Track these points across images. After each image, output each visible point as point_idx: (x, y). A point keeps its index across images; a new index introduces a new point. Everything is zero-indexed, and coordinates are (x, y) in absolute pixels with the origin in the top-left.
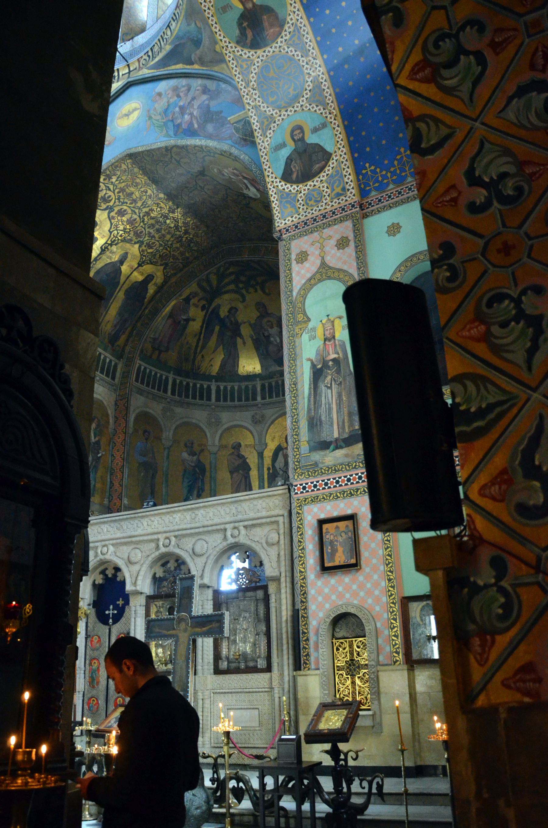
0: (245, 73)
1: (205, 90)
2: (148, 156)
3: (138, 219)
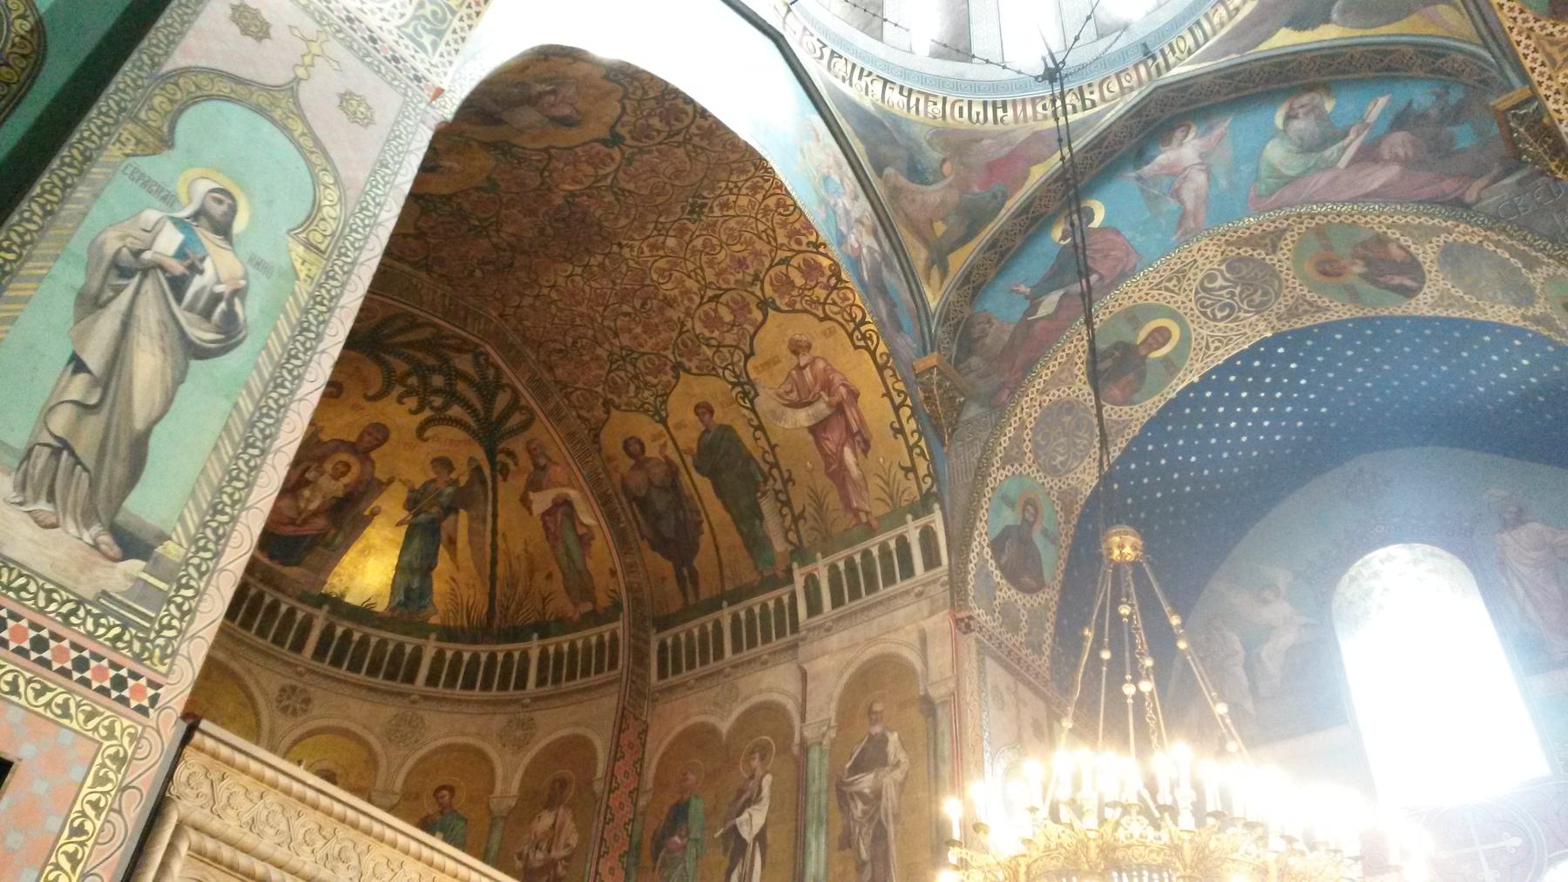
0: (1056, 381)
1: (875, 234)
2: (778, 205)
3: (578, 187)
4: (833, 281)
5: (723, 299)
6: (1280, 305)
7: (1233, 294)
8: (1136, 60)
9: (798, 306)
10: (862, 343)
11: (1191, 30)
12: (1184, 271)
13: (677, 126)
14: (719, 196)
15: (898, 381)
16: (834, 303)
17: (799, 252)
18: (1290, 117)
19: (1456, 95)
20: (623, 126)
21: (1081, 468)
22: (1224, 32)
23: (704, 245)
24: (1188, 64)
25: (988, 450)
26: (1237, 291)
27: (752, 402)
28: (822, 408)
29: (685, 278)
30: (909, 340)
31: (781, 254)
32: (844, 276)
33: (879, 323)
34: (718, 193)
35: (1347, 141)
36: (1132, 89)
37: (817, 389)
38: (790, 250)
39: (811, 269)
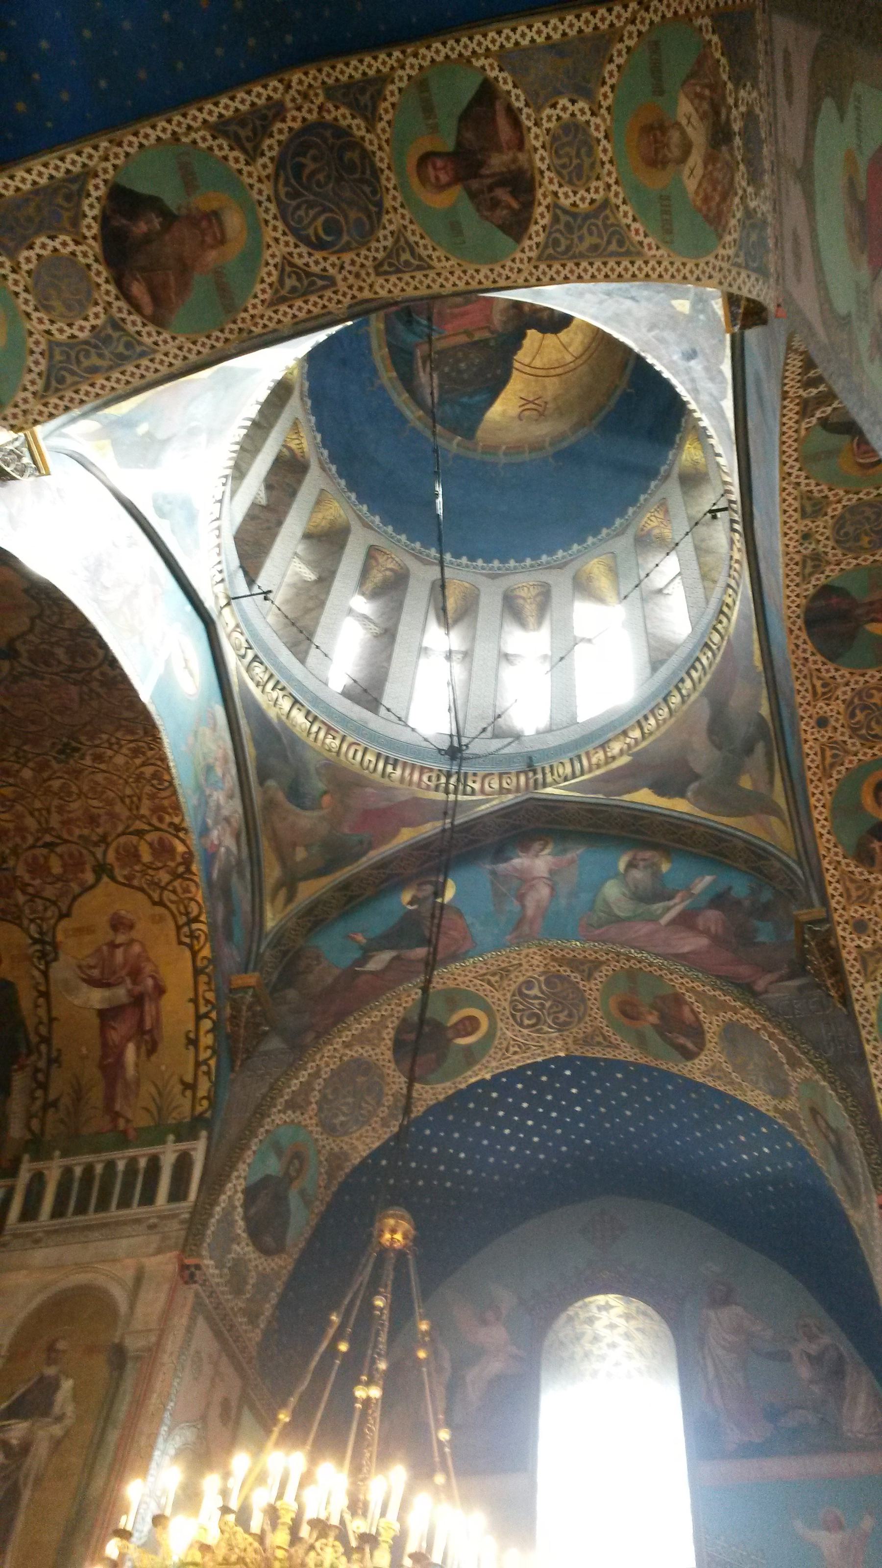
0: (362, 1039)
1: (237, 837)
2: (155, 776)
4: (181, 869)
5: (59, 850)
6: (577, 1031)
7: (542, 1005)
8: (519, 768)
9: (135, 883)
10: (187, 940)
11: (571, 760)
12: (508, 971)
13: (81, 663)
14: (97, 746)
15: (210, 990)
16: (174, 892)
17: (158, 829)
18: (631, 865)
19: (766, 895)
20: (24, 643)
21: (358, 1134)
22: (598, 772)
23: (63, 787)
24: (561, 788)
25: (274, 1090)
26: (548, 1004)
27: (47, 964)
28: (121, 994)
29: (27, 814)
30: (235, 953)
31: (139, 825)
32: (194, 868)
33: (212, 925)
34: (97, 742)
35: (671, 903)
36: (509, 791)
37: (123, 973)
38: (150, 824)
39: (163, 850)
